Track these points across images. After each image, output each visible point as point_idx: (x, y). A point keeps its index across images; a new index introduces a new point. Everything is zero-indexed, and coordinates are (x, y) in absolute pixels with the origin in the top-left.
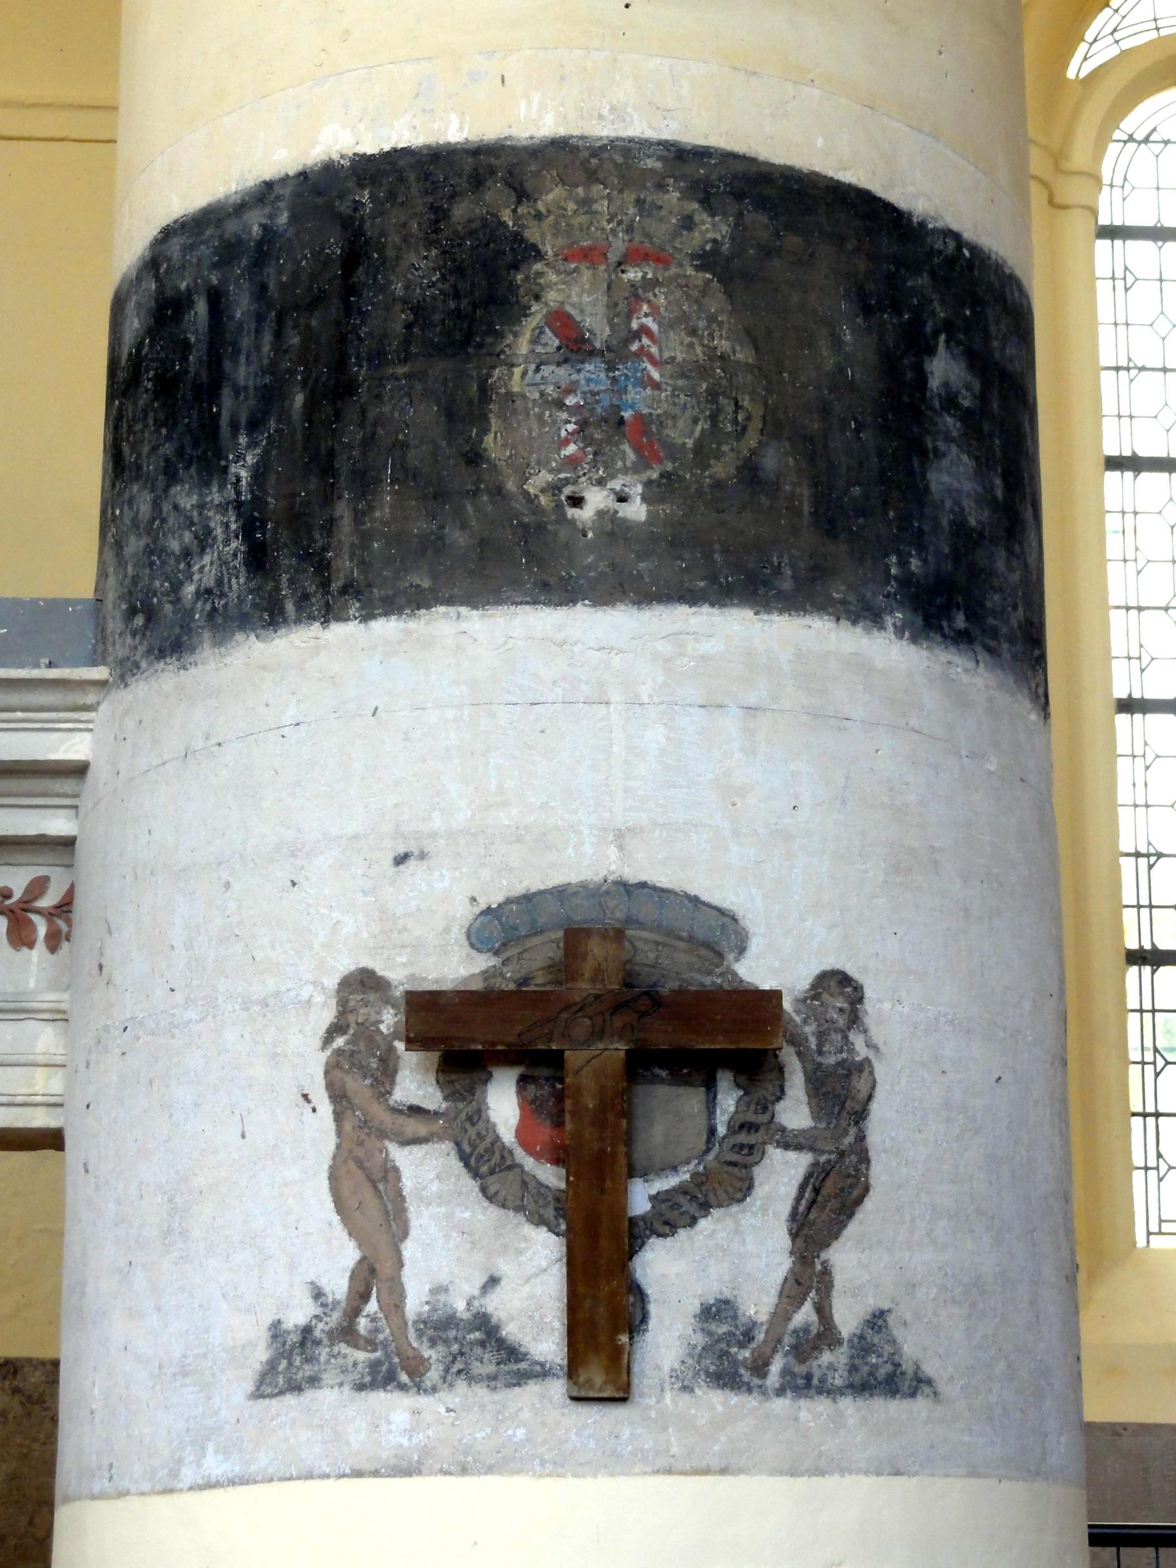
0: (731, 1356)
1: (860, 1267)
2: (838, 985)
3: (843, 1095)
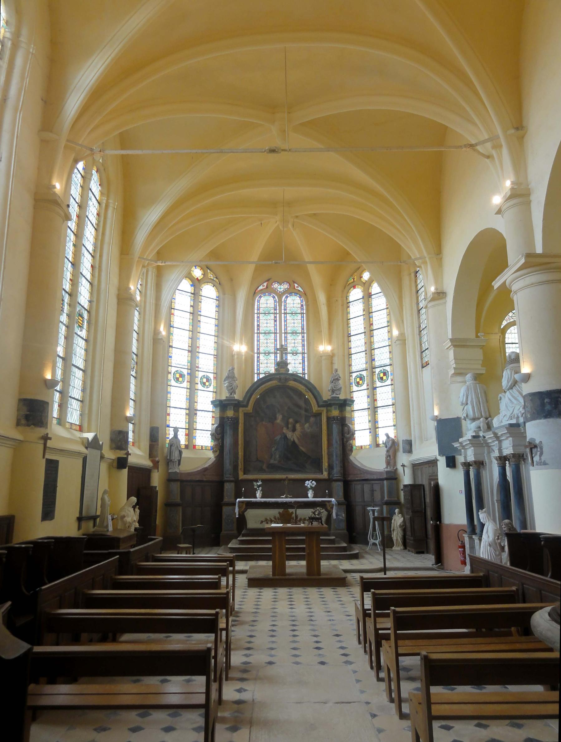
0: (537, 465)
1: (543, 458)
2: (541, 442)
3: (541, 449)
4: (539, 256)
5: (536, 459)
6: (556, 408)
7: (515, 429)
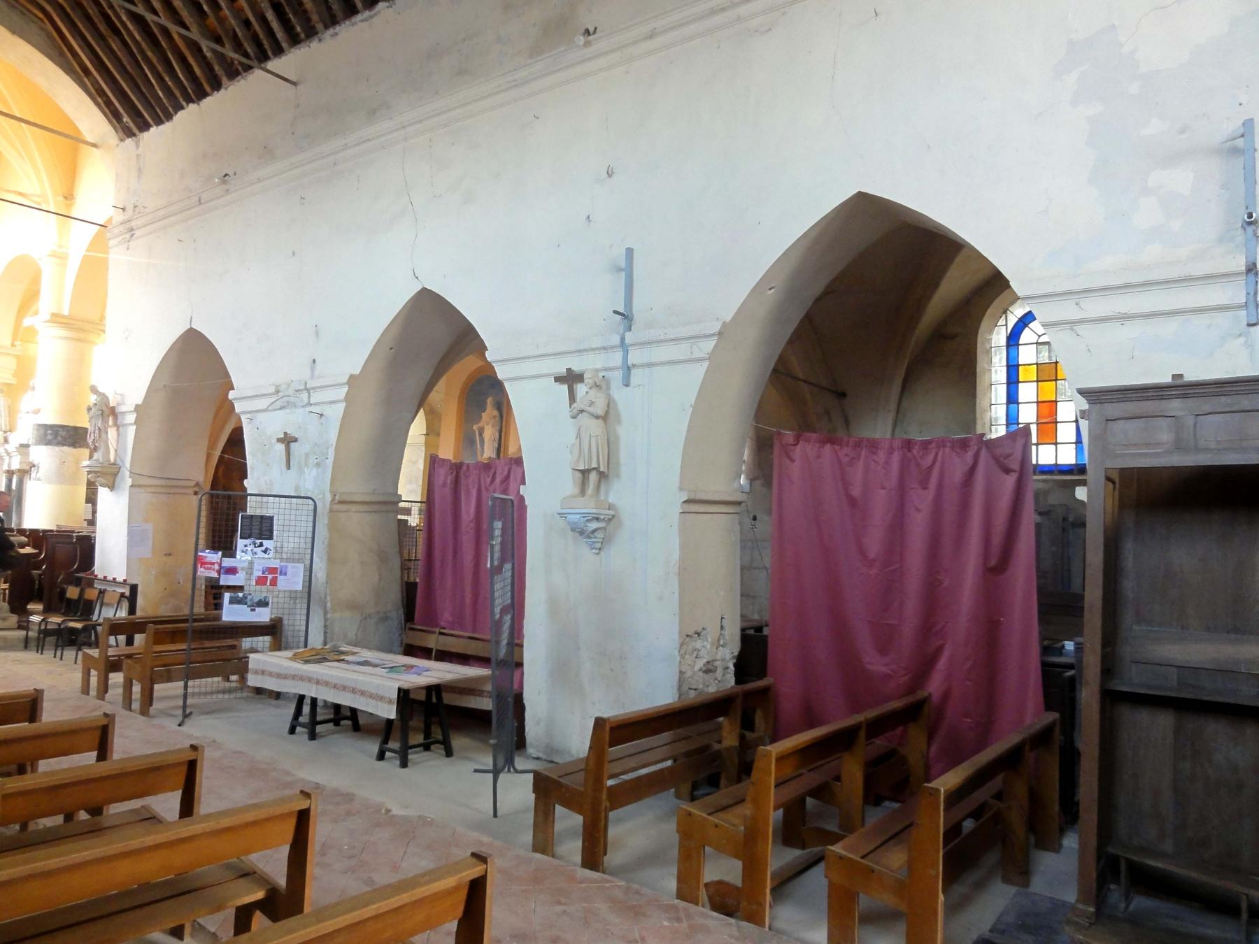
4: (63, 317)
5: (33, 475)
6: (56, 437)
7: (24, 447)
